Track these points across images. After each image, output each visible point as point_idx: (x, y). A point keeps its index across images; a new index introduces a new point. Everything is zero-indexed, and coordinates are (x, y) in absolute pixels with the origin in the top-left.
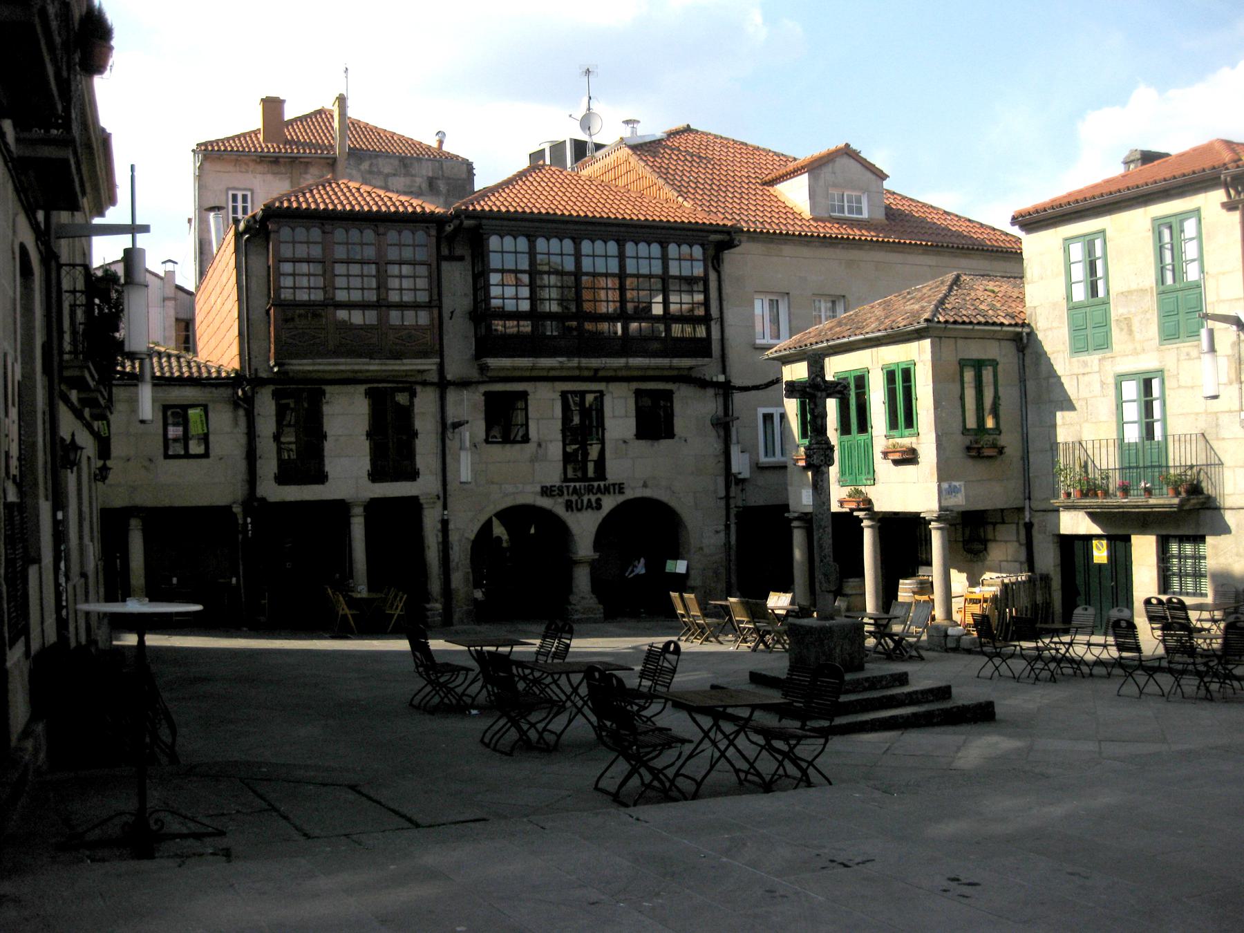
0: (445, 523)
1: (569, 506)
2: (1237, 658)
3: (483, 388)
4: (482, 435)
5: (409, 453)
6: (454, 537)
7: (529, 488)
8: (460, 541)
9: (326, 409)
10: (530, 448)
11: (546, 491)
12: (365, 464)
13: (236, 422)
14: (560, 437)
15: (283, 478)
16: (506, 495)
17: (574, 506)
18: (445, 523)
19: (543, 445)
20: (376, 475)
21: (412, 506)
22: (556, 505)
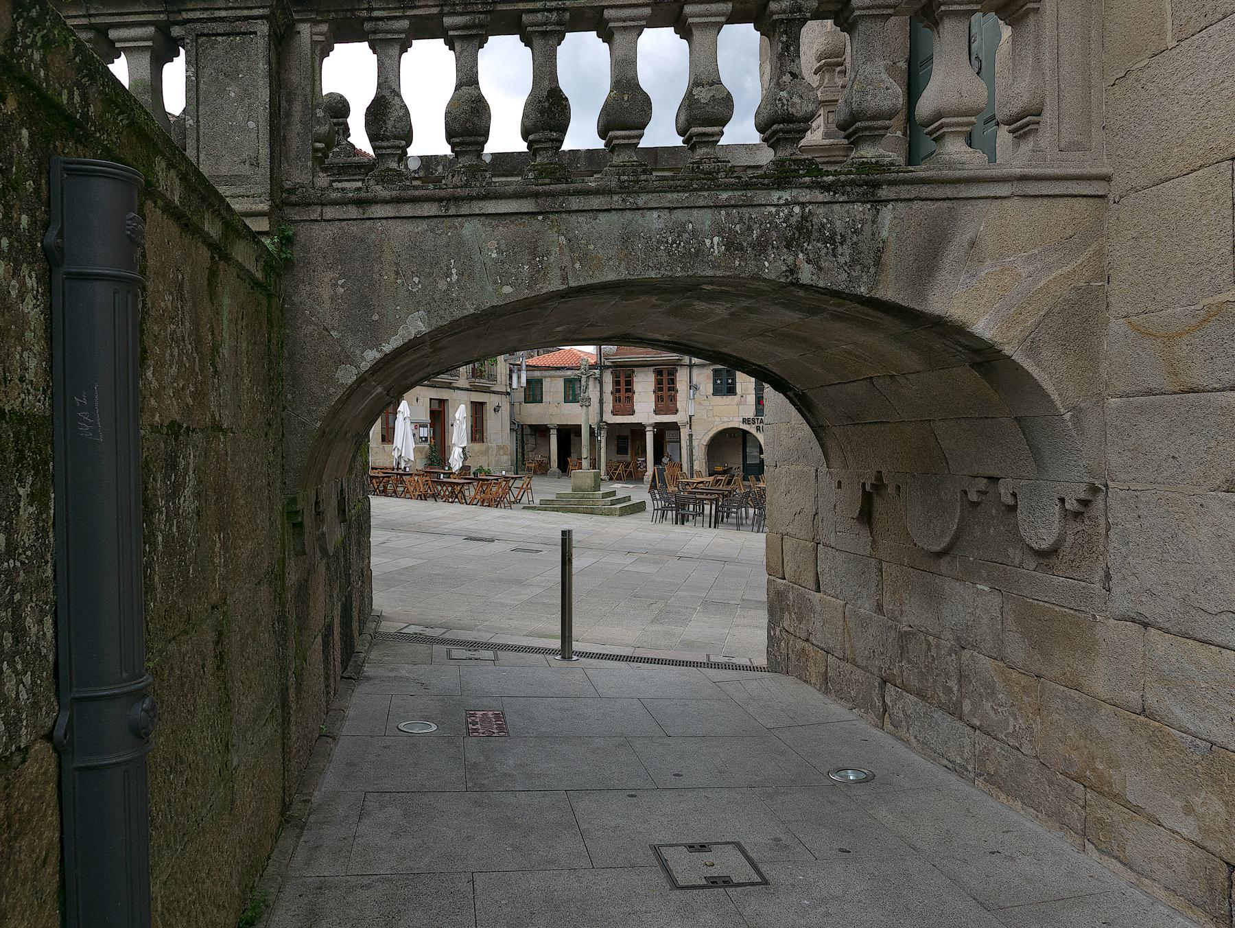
0: (691, 436)
1: (758, 429)
2: (658, 497)
3: (712, 368)
4: (711, 391)
5: (673, 399)
6: (695, 443)
7: (735, 419)
8: (698, 445)
9: (635, 379)
10: (736, 398)
11: (745, 421)
12: (653, 406)
13: (595, 387)
14: (754, 392)
15: (614, 413)
16: (724, 422)
17: (761, 429)
18: (691, 436)
19: (744, 396)
20: (656, 412)
21: (674, 427)
22: (751, 429)
